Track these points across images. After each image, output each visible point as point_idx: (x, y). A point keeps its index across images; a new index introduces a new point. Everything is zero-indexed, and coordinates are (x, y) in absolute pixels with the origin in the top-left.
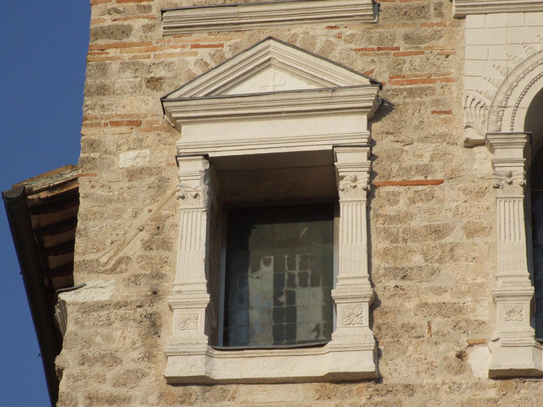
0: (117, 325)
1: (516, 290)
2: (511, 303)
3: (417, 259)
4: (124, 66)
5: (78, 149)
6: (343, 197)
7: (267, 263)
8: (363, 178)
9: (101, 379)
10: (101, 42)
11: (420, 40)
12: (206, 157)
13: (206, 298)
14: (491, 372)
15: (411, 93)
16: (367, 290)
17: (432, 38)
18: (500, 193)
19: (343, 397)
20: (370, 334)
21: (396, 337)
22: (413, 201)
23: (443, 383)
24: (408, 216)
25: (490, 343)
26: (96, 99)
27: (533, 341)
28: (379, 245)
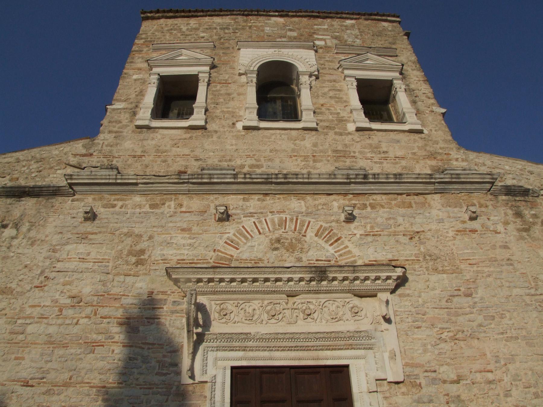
0: (123, 113)
1: (252, 106)
2: (251, 110)
3: (222, 100)
4: (139, 58)
5: (121, 74)
6: (199, 84)
7: (176, 110)
8: (206, 80)
9: (114, 127)
10: (134, 53)
11: (227, 54)
12: (159, 74)
13: (152, 106)
14: (243, 127)
15: (223, 64)
16: (205, 105)
17: (230, 53)
18: (248, 84)
19: (194, 133)
20: (204, 117)
21: (213, 119)
22: (221, 87)
23: (227, 130)
24: (219, 90)
25: (244, 120)
26: (129, 64)
27: (257, 119)
28: (210, 96)
